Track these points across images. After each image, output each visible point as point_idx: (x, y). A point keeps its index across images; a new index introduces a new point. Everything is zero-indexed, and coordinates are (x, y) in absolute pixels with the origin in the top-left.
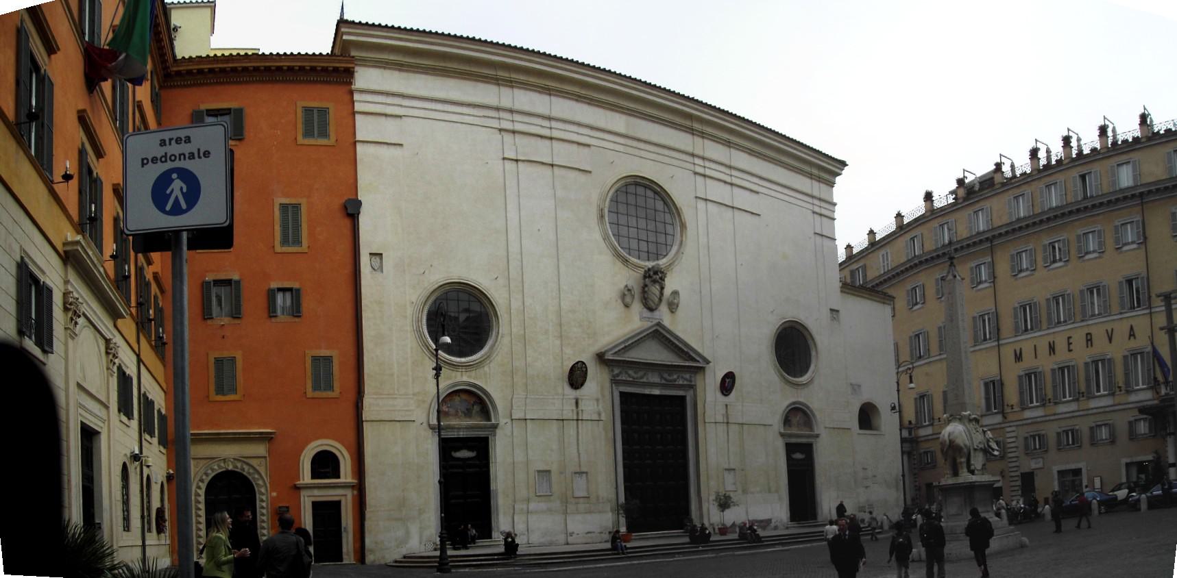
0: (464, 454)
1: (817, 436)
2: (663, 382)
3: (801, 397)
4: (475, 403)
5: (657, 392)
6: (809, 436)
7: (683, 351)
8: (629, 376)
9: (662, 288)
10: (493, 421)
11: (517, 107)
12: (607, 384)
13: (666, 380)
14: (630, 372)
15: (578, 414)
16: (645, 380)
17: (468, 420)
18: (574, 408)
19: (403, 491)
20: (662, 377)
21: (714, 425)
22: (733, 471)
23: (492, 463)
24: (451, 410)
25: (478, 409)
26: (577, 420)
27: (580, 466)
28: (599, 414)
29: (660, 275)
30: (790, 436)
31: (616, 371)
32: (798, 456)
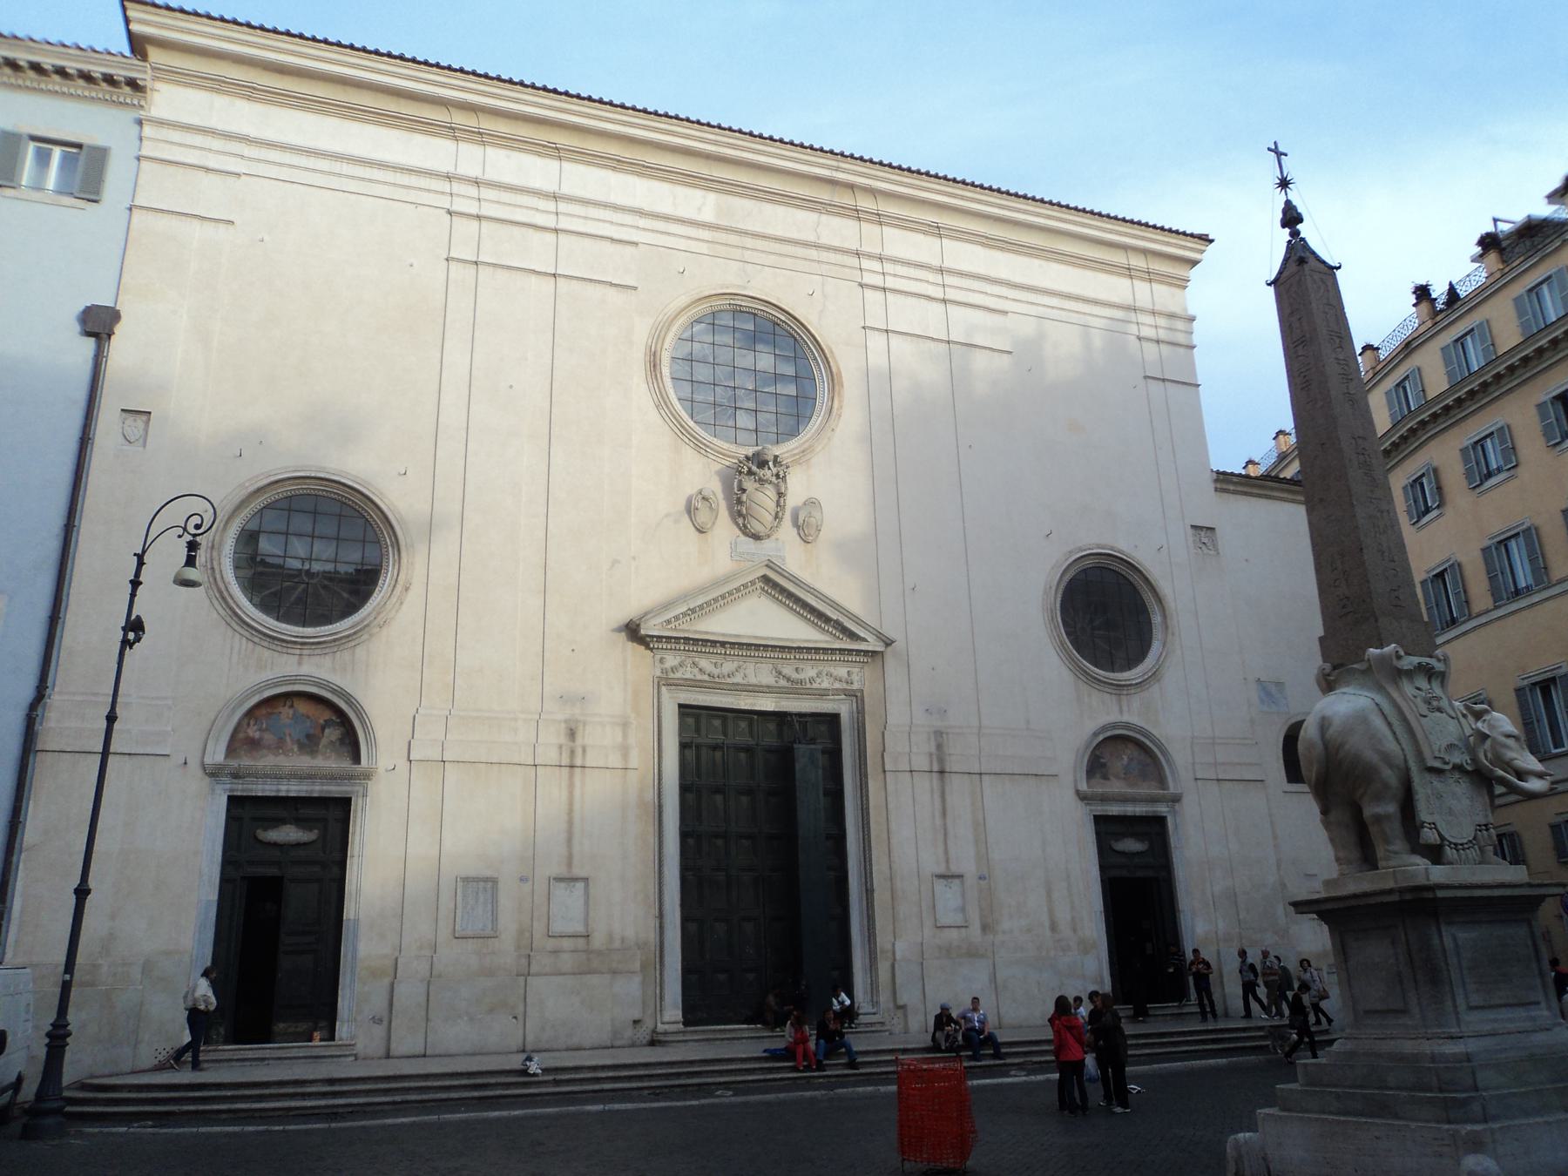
0: (289, 834)
1: (1176, 799)
2: (783, 683)
3: (1131, 713)
4: (328, 723)
5: (767, 704)
6: (1154, 800)
7: (827, 620)
9: (780, 495)
11: (491, 175)
12: (648, 690)
13: (788, 679)
14: (704, 663)
15: (572, 752)
16: (738, 679)
18: (563, 740)
19: (113, 917)
21: (908, 774)
22: (957, 881)
23: (352, 856)
24: (269, 738)
25: (333, 738)
26: (572, 767)
27: (570, 865)
28: (625, 750)
29: (774, 470)
30: (1104, 799)
31: (671, 660)
32: (1131, 845)
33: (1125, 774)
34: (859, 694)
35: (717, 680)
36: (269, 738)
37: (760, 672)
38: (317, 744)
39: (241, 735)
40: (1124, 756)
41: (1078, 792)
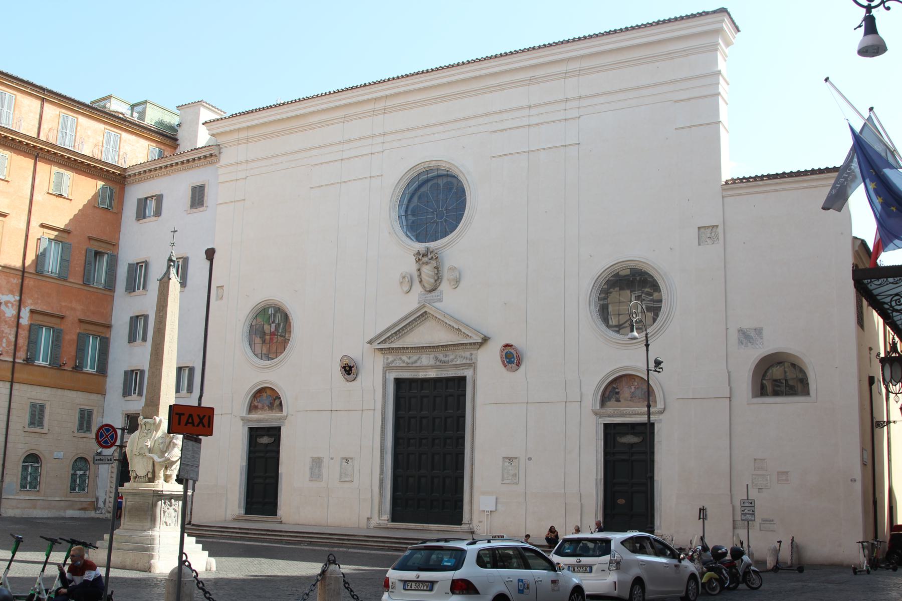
0: (265, 440)
2: (438, 363)
5: (432, 374)
8: (404, 362)
10: (284, 412)
14: (404, 358)
16: (418, 364)
17: (270, 412)
20: (437, 358)
25: (278, 403)
29: (430, 256)
31: (391, 358)
33: (631, 397)
34: (473, 365)
35: (409, 365)
36: (260, 405)
37: (426, 359)
38: (273, 406)
39: (253, 405)
40: (632, 387)
41: (592, 410)
